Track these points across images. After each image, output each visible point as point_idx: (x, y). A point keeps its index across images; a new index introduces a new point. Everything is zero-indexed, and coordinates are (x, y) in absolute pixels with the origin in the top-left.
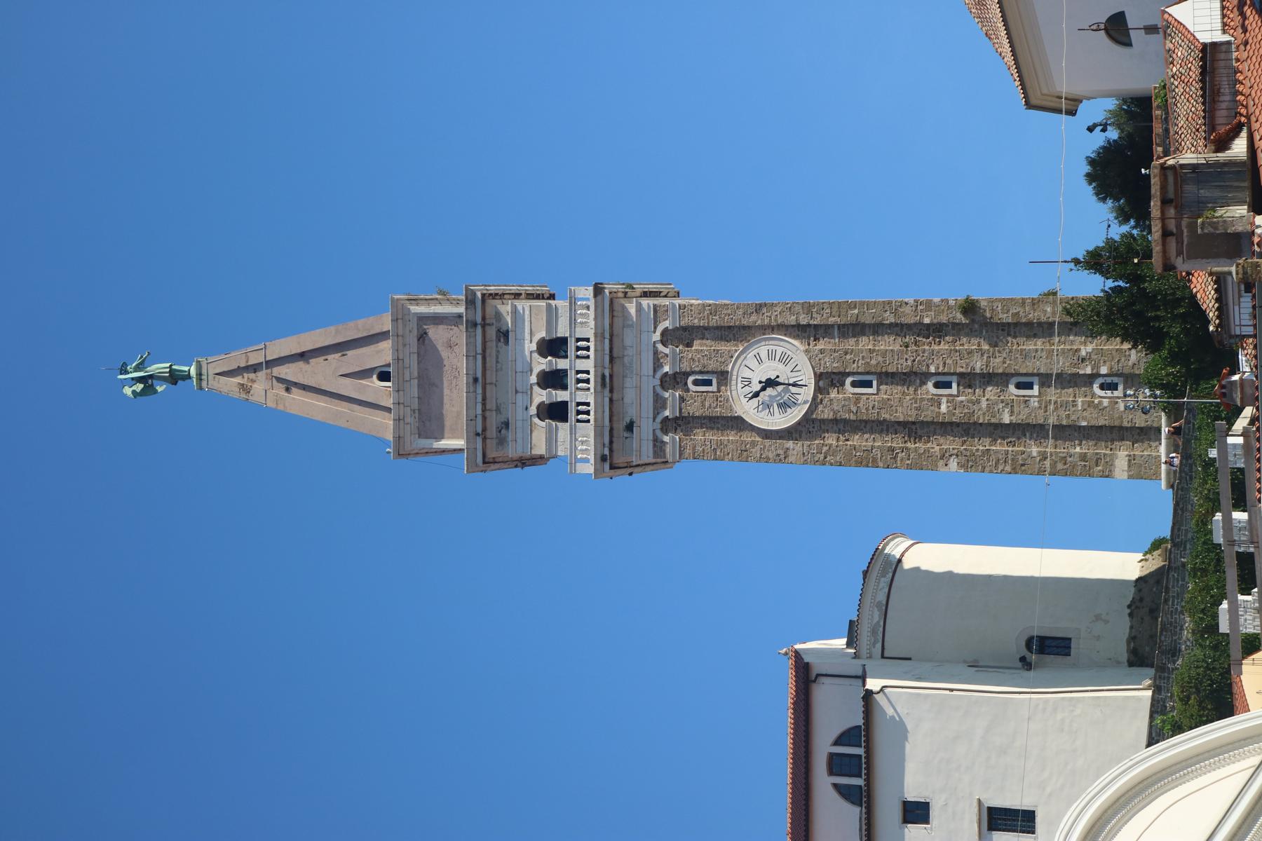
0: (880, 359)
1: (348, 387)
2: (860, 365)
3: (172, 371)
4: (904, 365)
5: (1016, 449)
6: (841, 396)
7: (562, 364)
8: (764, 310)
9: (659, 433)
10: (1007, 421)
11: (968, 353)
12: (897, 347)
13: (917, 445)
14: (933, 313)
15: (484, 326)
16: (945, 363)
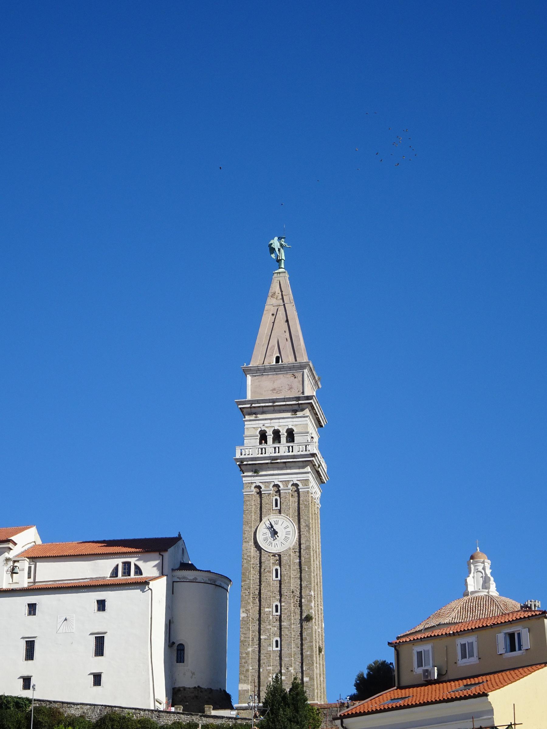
0: (287, 581)
1: (273, 342)
2: (284, 572)
3: (281, 260)
4: (284, 591)
5: (251, 642)
6: (271, 565)
7: (283, 439)
8: (307, 529)
9: (254, 485)
10: (262, 637)
11: (290, 619)
12: (292, 588)
13: (251, 598)
14: (306, 603)
15: (298, 404)
16: (285, 609)
